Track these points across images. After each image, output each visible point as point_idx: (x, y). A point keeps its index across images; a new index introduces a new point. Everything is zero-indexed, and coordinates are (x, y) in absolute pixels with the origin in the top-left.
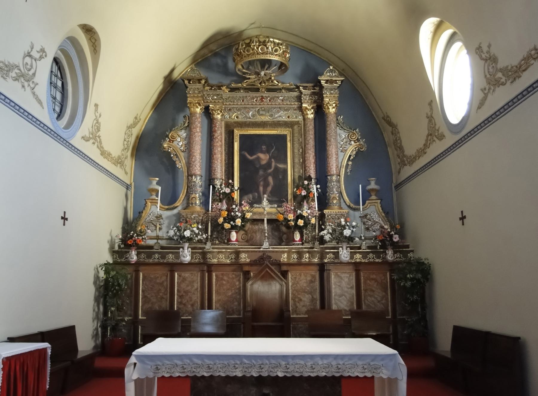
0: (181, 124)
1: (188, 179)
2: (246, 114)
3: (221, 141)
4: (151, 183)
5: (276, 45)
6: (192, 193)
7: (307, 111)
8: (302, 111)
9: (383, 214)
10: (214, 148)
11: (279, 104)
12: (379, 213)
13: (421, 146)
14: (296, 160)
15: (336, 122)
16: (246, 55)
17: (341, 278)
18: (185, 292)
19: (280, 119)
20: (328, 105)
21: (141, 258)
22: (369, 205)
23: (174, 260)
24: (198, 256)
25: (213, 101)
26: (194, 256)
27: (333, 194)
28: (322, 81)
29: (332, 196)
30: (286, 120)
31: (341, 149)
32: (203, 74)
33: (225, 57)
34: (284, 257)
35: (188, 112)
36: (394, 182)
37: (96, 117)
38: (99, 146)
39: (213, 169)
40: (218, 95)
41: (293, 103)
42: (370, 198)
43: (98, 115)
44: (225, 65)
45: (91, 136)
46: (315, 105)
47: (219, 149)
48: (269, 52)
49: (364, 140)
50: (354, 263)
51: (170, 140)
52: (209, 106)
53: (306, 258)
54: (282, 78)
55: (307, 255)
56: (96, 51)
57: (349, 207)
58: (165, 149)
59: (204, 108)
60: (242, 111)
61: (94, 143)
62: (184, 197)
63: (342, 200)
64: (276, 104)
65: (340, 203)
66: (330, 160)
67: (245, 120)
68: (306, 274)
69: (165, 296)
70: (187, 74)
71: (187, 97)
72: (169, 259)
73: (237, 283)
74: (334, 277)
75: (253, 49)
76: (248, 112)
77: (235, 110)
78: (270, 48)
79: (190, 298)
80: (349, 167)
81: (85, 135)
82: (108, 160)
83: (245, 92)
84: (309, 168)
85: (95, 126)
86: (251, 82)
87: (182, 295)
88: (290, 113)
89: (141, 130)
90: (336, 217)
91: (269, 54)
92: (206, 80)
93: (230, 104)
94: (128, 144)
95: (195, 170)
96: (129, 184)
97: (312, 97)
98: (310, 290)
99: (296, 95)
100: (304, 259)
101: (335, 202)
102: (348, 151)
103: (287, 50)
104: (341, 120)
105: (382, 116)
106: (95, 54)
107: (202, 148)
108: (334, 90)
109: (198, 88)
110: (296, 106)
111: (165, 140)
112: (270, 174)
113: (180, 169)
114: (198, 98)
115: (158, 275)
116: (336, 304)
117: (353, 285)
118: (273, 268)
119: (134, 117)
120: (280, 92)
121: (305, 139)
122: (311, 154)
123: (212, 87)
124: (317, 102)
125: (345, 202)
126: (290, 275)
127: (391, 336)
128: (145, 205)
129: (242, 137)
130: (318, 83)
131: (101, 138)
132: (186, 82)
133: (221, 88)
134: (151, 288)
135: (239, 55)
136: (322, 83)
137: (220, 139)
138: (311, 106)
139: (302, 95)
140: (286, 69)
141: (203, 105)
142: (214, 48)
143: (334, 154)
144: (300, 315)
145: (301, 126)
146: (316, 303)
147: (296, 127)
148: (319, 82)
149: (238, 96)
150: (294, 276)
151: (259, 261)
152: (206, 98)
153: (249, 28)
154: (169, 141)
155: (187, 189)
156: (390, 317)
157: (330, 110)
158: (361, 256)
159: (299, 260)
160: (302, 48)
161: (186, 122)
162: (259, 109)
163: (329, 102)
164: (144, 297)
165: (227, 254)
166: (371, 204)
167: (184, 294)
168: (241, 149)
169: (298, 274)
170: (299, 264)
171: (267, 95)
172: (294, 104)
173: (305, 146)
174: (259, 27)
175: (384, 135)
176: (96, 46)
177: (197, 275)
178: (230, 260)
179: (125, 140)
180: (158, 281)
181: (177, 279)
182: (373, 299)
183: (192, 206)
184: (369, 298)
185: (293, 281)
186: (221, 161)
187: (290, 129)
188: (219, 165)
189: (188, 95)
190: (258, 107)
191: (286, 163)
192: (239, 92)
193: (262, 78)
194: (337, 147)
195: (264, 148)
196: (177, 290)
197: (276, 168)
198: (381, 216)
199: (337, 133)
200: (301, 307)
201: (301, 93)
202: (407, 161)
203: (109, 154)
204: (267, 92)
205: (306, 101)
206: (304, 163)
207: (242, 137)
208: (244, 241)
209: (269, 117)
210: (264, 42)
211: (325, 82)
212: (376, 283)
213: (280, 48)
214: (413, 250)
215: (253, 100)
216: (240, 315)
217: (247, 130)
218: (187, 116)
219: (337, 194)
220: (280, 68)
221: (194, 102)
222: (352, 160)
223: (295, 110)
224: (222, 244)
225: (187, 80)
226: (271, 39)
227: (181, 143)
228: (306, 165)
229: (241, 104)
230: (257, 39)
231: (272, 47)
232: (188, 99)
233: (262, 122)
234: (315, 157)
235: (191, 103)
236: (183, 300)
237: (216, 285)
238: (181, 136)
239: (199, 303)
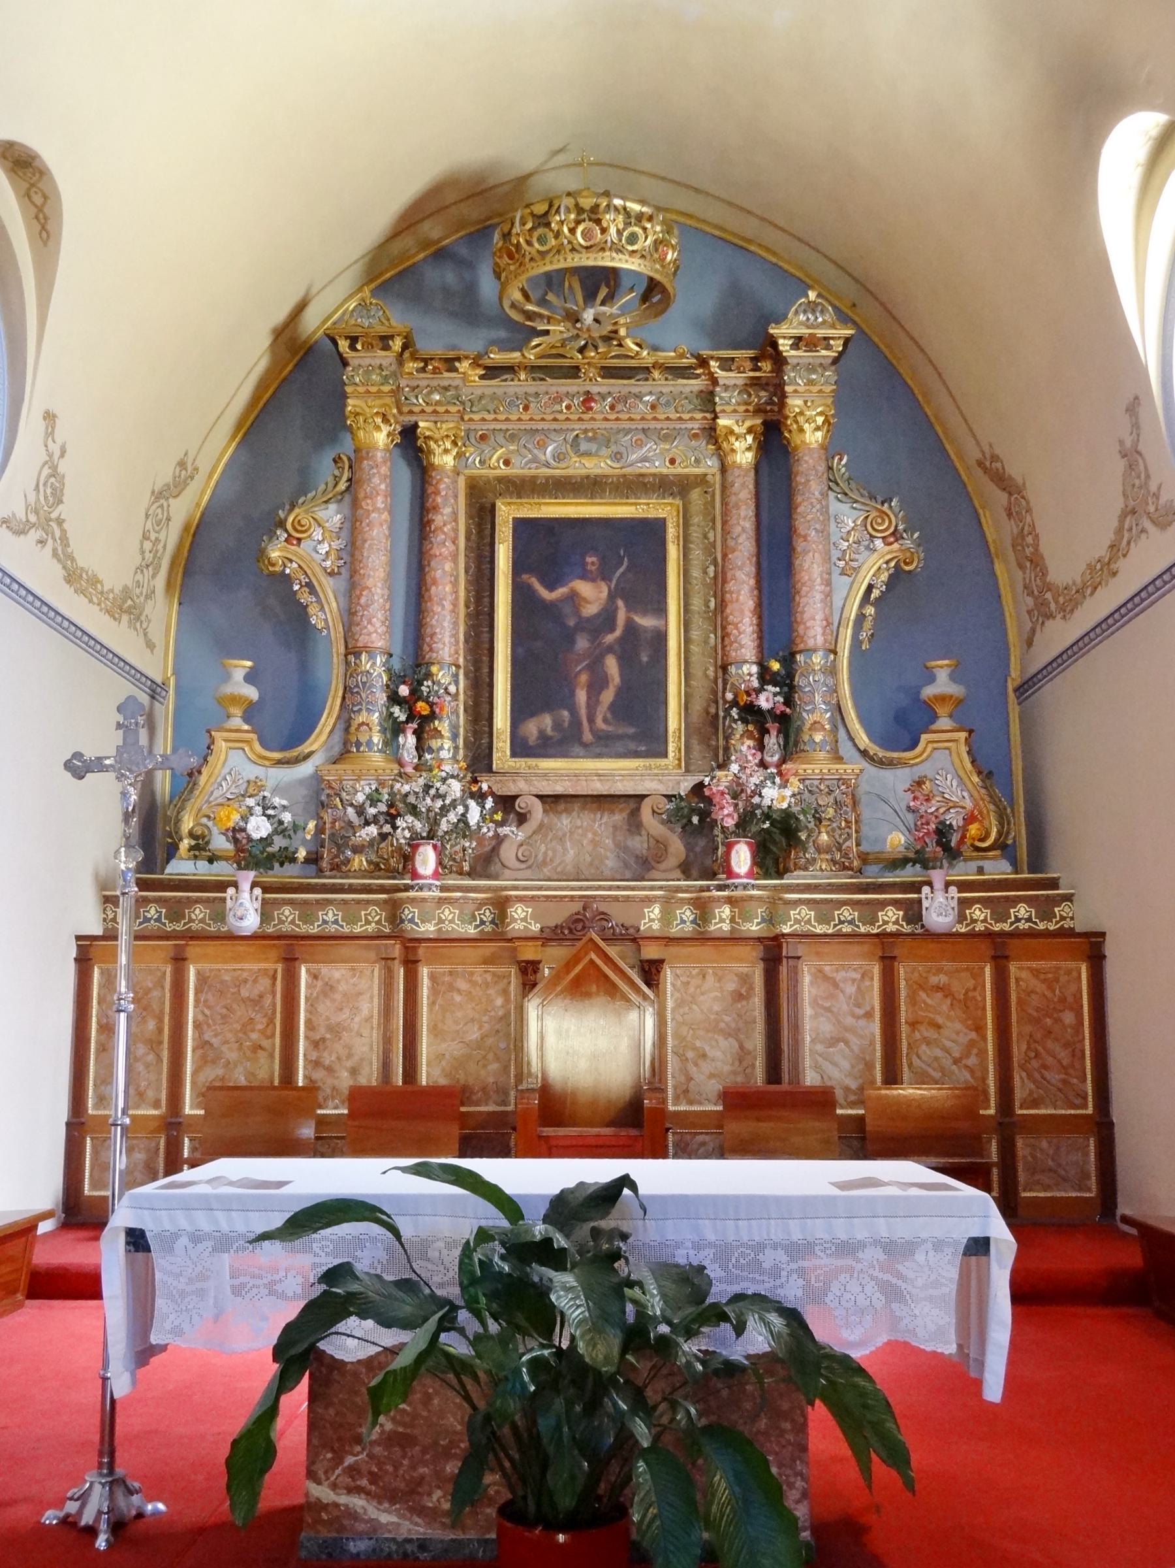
0: (327, 484)
1: (347, 663)
2: (536, 451)
3: (454, 541)
4: (227, 677)
5: (633, 220)
6: (360, 710)
7: (732, 439)
8: (717, 442)
9: (976, 779)
10: (433, 563)
11: (643, 419)
12: (961, 773)
13: (1102, 551)
14: (697, 603)
15: (825, 476)
16: (534, 252)
17: (836, 985)
18: (330, 1029)
19: (647, 468)
20: (801, 419)
21: (193, 921)
22: (929, 749)
23: (298, 926)
24: (374, 914)
25: (429, 409)
26: (363, 913)
27: (812, 711)
28: (781, 341)
29: (809, 719)
30: (665, 471)
31: (842, 564)
32: (397, 318)
33: (470, 265)
34: (652, 916)
35: (346, 447)
36: (1013, 674)
37: (50, 455)
38: (60, 552)
39: (428, 630)
40: (446, 389)
41: (686, 416)
42: (933, 727)
43: (55, 448)
44: (471, 289)
45: (33, 518)
46: (758, 421)
47: (448, 566)
48: (609, 244)
49: (916, 535)
50: (877, 935)
51: (290, 535)
52: (416, 426)
53: (722, 920)
54: (656, 330)
55: (726, 911)
56: (48, 236)
57: (864, 753)
58: (273, 565)
59: (400, 433)
60: (523, 442)
61: (41, 542)
62: (332, 721)
63: (842, 733)
64: (632, 420)
65: (837, 742)
66: (804, 600)
67: (533, 472)
68: (720, 973)
69: (266, 1043)
70: (346, 318)
71: (344, 396)
72: (281, 922)
73: (499, 1002)
74: (812, 983)
75: (557, 235)
76: (542, 446)
77: (500, 439)
78: (613, 230)
79: (349, 1047)
80: (868, 624)
81: (14, 515)
82: (91, 601)
83: (534, 379)
84: (737, 628)
85: (45, 484)
86: (553, 347)
87: (323, 1040)
88: (677, 448)
89: (198, 505)
90: (822, 787)
91: (610, 249)
92: (406, 337)
93: (483, 420)
94: (157, 551)
95: (369, 634)
96: (159, 680)
97: (750, 395)
98: (733, 1025)
99: (696, 389)
100: (716, 924)
101: (818, 737)
102: (863, 572)
103: (667, 236)
104: (843, 470)
105: (979, 456)
106: (45, 244)
107: (391, 563)
108: (820, 370)
109: (381, 367)
110: (697, 426)
111: (272, 535)
112: (610, 649)
113: (320, 631)
114: (380, 397)
115: (245, 975)
116: (817, 1067)
117: (873, 1008)
118: (612, 951)
119: (178, 459)
120: (647, 379)
121: (726, 532)
122: (744, 582)
123: (426, 361)
124: (766, 412)
125: (852, 739)
126: (668, 975)
127: (995, 1171)
128: (209, 748)
129: (522, 526)
130: (769, 349)
131: (65, 526)
132: (343, 345)
133: (457, 364)
134: (224, 1017)
135: (514, 253)
136: (781, 348)
137: (452, 534)
138: (748, 424)
139: (718, 389)
140: (667, 299)
141: (397, 422)
142: (435, 234)
143: (819, 580)
144: (700, 1103)
145: (714, 491)
146: (753, 1066)
147: (695, 495)
148: (774, 344)
149: (511, 391)
150: (684, 979)
151: (571, 931)
152: (406, 399)
153: (550, 165)
154: (286, 540)
155: (344, 698)
156: (992, 1112)
157: (807, 435)
158: (901, 913)
159: (699, 925)
160: (717, 233)
161: (340, 478)
162: (577, 435)
163: (805, 408)
164: (202, 1045)
165: (471, 907)
166: (935, 745)
167: (328, 1036)
168: (518, 567)
169: (694, 972)
170: (701, 938)
171: (604, 390)
172: (692, 419)
173: (725, 556)
174: (581, 165)
175: (983, 520)
176: (46, 218)
177: (368, 973)
178: (477, 927)
179: (145, 537)
180: (245, 993)
181: (308, 986)
182: (938, 1052)
183: (358, 751)
184: (924, 1047)
185: (677, 995)
186: (455, 605)
187: (678, 502)
188: (448, 618)
189: (348, 389)
190: (573, 430)
191: (661, 610)
192: (512, 380)
193: (588, 330)
194: (827, 558)
195: (593, 563)
196: (306, 1023)
197: (631, 629)
198: (970, 786)
199: (827, 512)
200: (702, 1077)
201: (714, 381)
202: (1057, 602)
203: (94, 581)
204: (603, 377)
205: (729, 409)
206: (722, 612)
207: (522, 526)
208: (523, 866)
209: (609, 462)
210: (595, 209)
211: (790, 342)
212: (949, 1001)
213: (645, 229)
214: (1072, 895)
215: (557, 407)
216: (505, 1103)
217: (540, 504)
218: (345, 459)
219: (826, 711)
220: (645, 297)
221: (367, 410)
222: (878, 603)
223: (695, 436)
224: (454, 875)
225: (347, 338)
226: (617, 202)
227: (326, 546)
228: (727, 617)
229: (520, 420)
230: (569, 202)
231: (621, 226)
232: (350, 401)
233: (588, 477)
234: (756, 592)
235: (358, 414)
236: (326, 1054)
237: (432, 1004)
238: (327, 525)
239: (375, 1067)
